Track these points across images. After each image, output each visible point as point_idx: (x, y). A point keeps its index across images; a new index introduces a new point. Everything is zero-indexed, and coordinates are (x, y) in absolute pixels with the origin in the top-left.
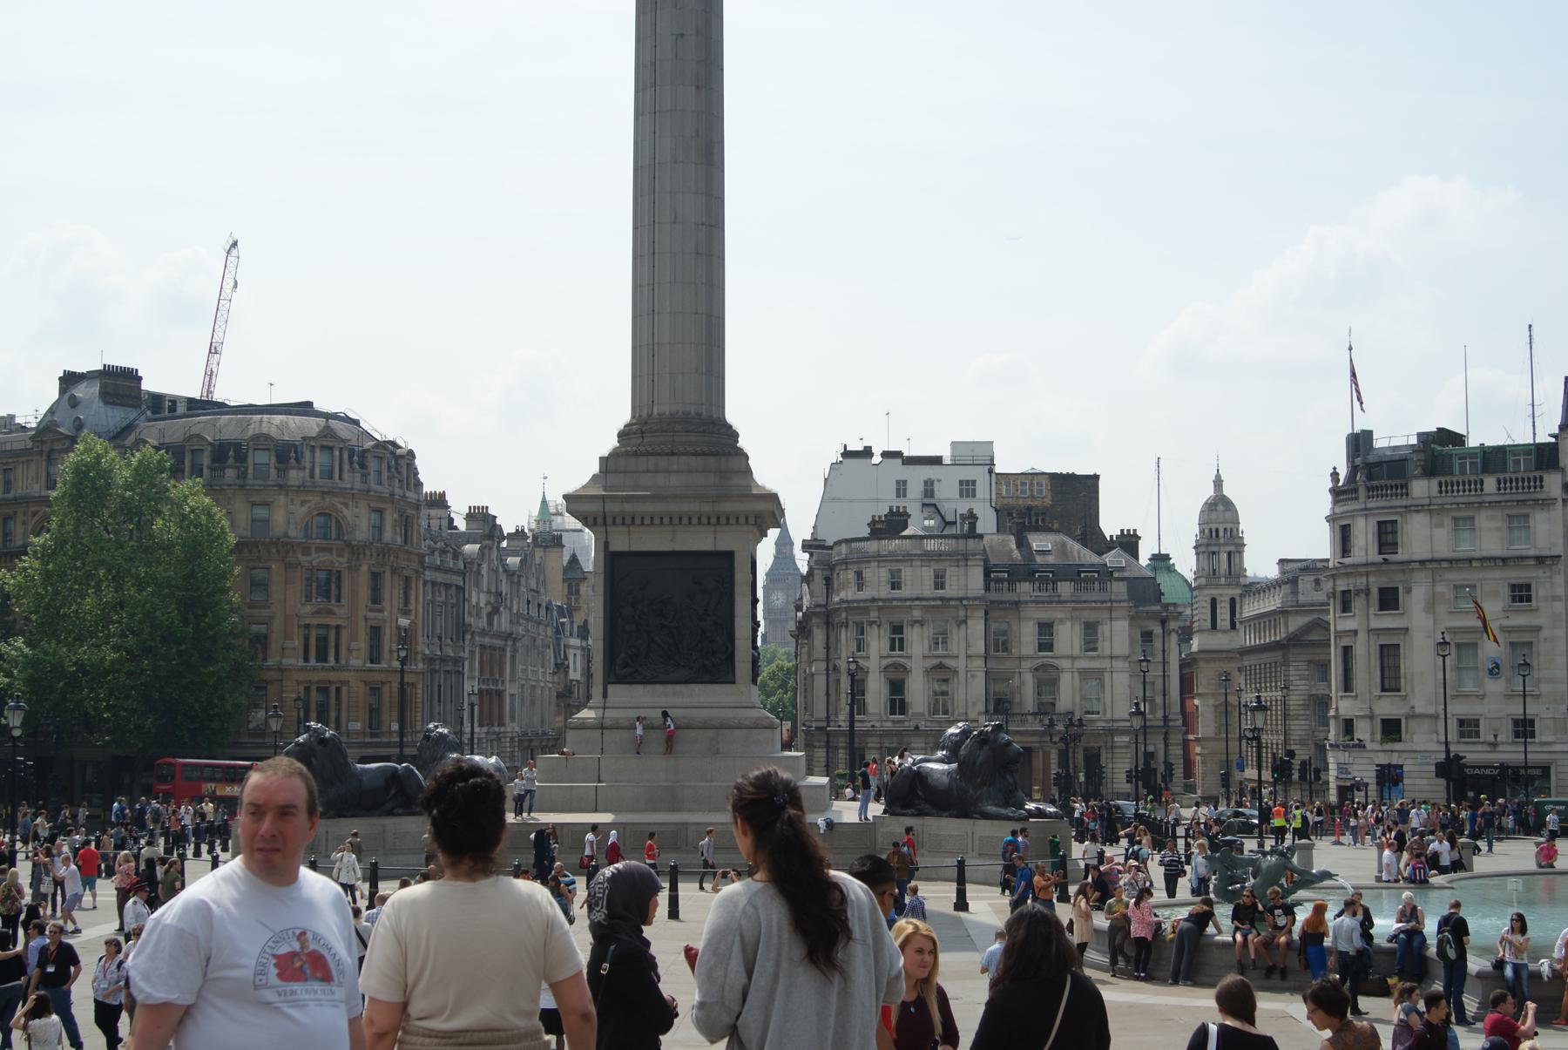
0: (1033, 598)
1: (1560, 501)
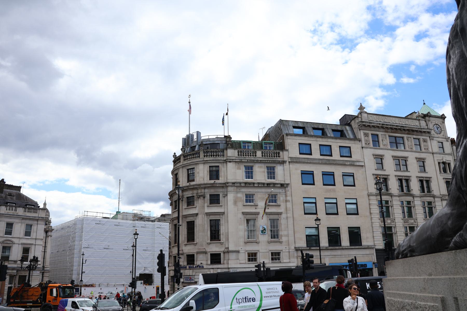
0: (6, 213)
1: (288, 163)
